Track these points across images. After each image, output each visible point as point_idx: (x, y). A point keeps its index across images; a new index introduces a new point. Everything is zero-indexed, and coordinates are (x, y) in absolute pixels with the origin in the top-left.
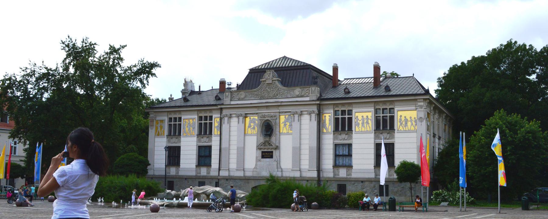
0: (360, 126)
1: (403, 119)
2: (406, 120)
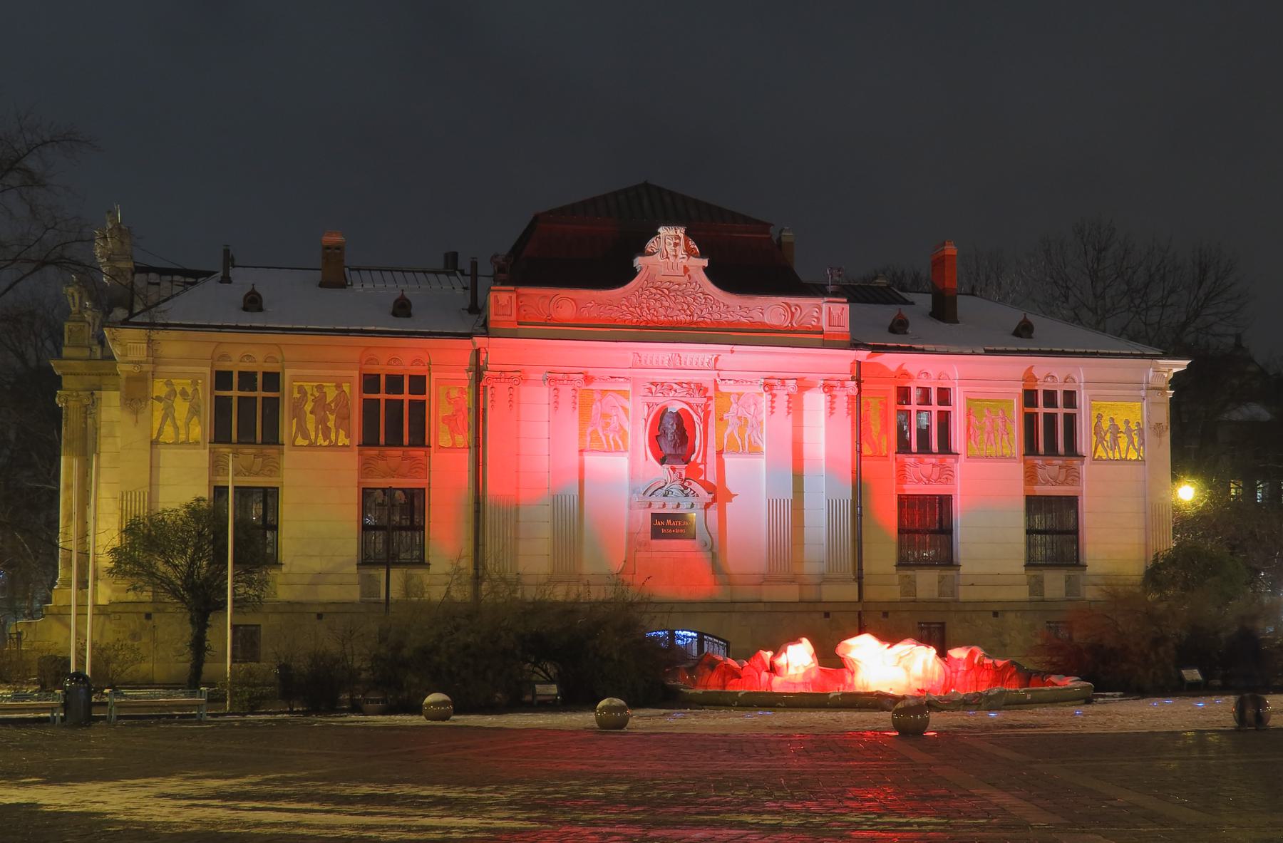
2: (1115, 430)
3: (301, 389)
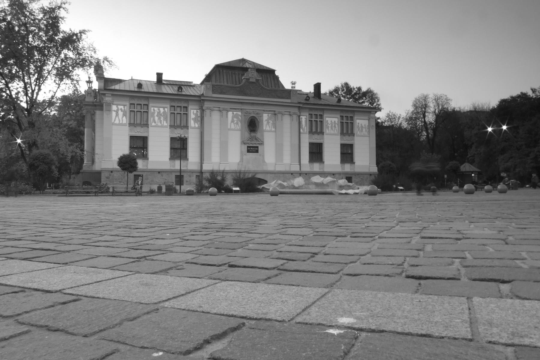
0: (330, 129)
1: (360, 126)
2: (362, 127)
3: (154, 110)
